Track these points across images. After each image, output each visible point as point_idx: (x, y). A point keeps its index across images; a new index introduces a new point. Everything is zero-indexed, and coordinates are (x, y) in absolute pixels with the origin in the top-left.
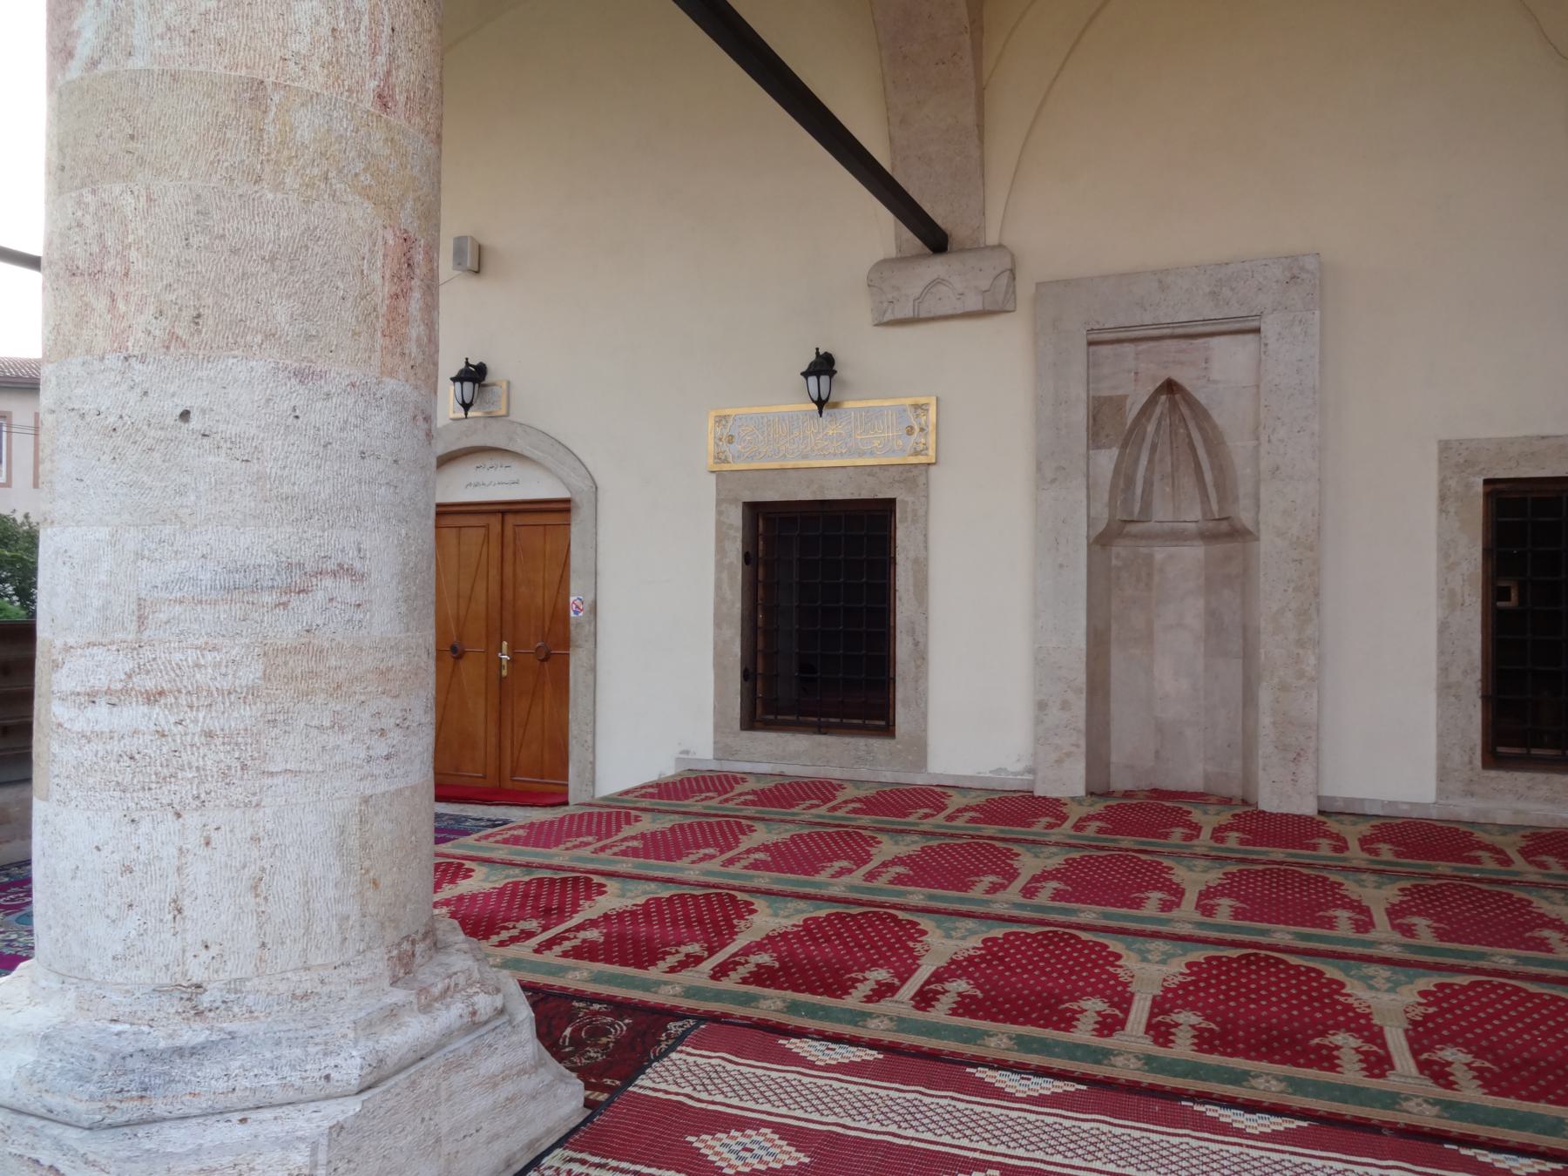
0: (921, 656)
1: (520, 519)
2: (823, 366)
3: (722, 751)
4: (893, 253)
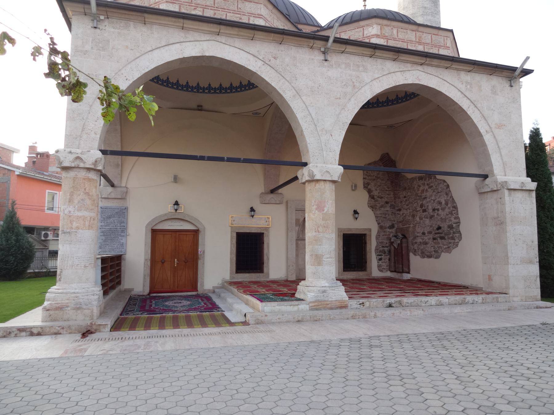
0: (268, 259)
1: (180, 233)
2: (252, 210)
3: (231, 277)
4: (264, 192)
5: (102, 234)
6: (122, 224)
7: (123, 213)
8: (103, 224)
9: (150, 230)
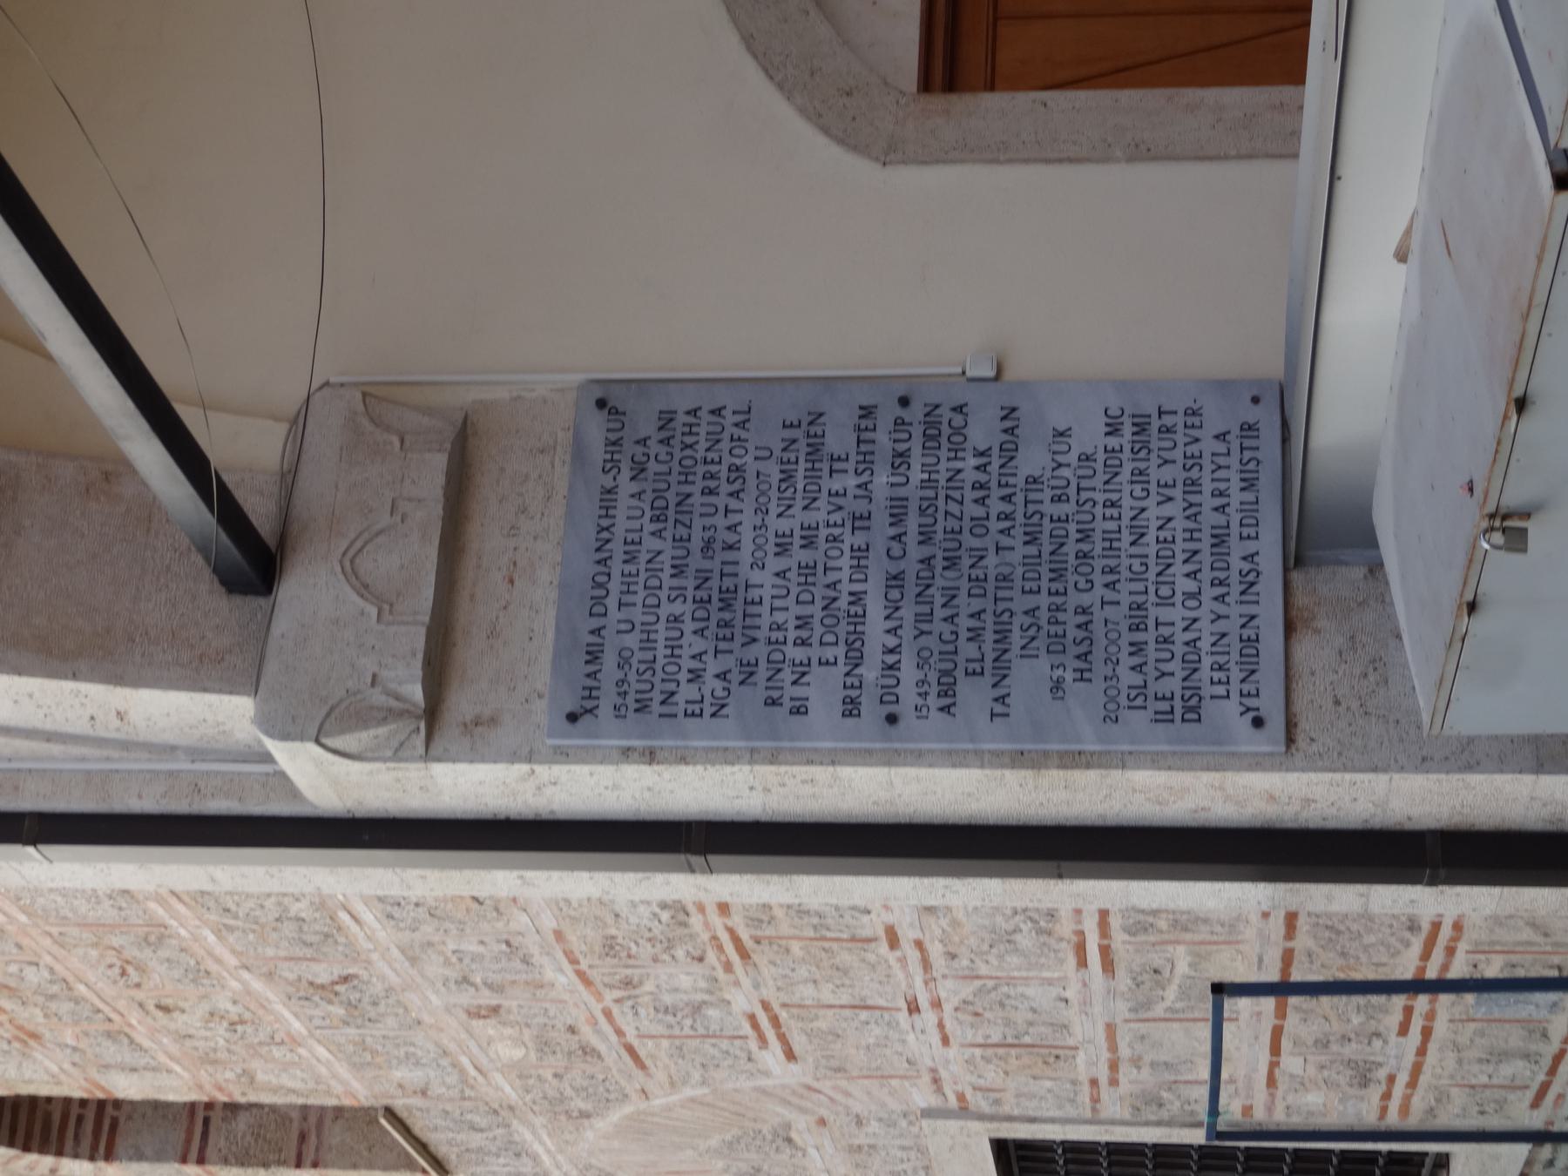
5: (973, 695)
6: (839, 439)
7: (665, 451)
8: (823, 690)
9: (938, 101)
